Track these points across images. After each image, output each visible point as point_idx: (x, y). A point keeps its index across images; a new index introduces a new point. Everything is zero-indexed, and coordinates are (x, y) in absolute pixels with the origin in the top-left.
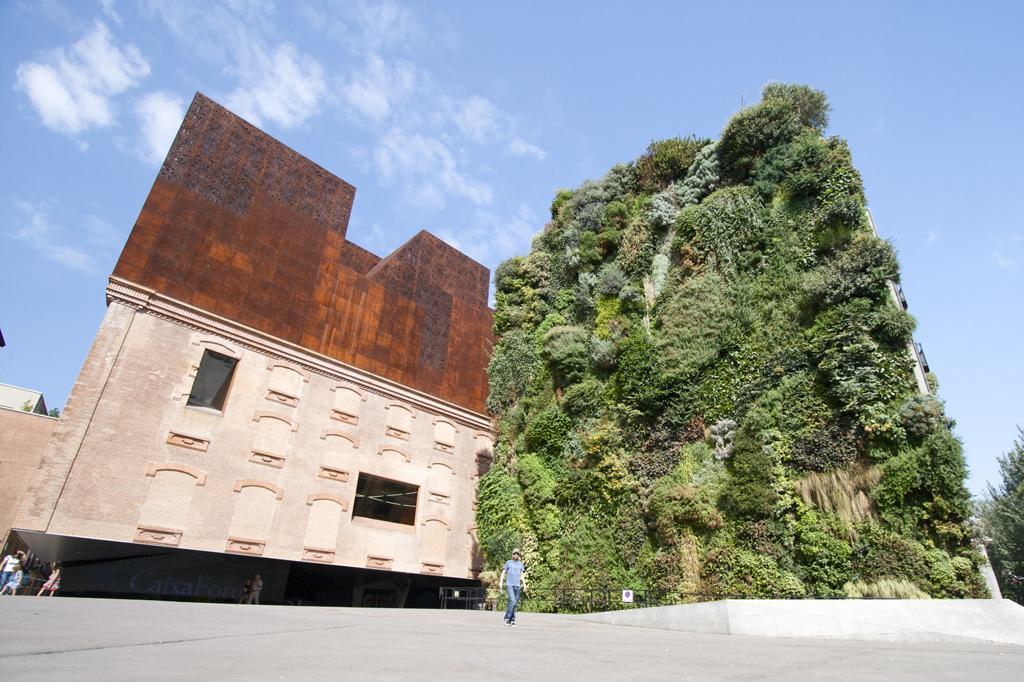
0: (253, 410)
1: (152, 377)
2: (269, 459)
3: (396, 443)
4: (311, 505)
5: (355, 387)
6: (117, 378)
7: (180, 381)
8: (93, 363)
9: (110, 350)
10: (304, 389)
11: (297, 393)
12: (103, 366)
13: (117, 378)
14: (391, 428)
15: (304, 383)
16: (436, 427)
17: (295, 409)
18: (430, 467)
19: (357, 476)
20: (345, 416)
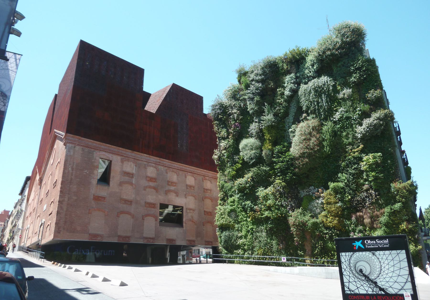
0: (119, 182)
1: (85, 174)
2: (128, 202)
3: (172, 188)
4: (144, 219)
5: (154, 165)
6: (74, 176)
7: (94, 174)
8: (66, 171)
9: (70, 164)
10: (135, 169)
11: (134, 172)
12: (69, 172)
13: (74, 176)
14: (170, 182)
15: (135, 167)
16: (187, 178)
17: (134, 179)
18: (186, 198)
19: (159, 205)
20: (151, 179)
